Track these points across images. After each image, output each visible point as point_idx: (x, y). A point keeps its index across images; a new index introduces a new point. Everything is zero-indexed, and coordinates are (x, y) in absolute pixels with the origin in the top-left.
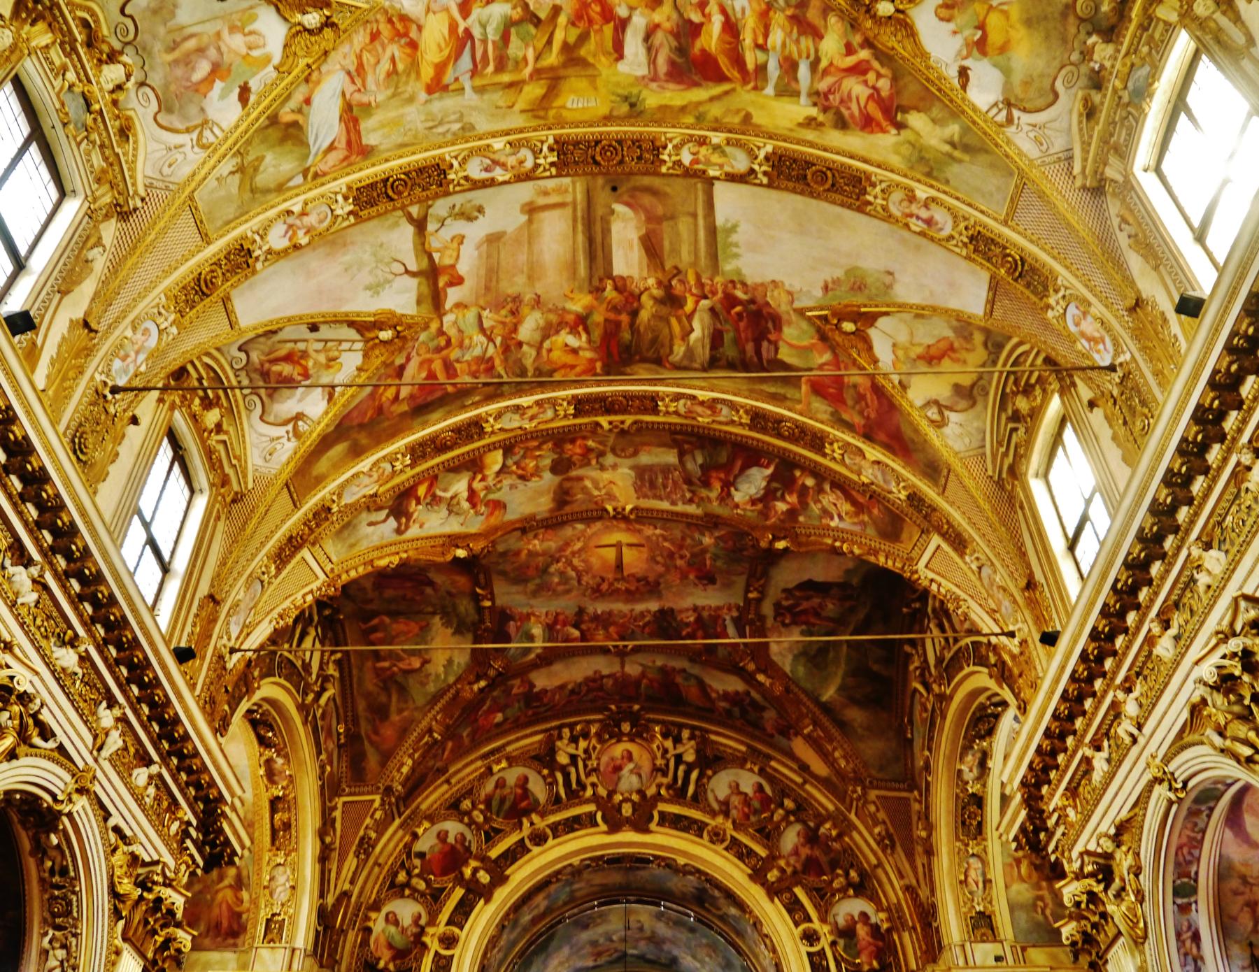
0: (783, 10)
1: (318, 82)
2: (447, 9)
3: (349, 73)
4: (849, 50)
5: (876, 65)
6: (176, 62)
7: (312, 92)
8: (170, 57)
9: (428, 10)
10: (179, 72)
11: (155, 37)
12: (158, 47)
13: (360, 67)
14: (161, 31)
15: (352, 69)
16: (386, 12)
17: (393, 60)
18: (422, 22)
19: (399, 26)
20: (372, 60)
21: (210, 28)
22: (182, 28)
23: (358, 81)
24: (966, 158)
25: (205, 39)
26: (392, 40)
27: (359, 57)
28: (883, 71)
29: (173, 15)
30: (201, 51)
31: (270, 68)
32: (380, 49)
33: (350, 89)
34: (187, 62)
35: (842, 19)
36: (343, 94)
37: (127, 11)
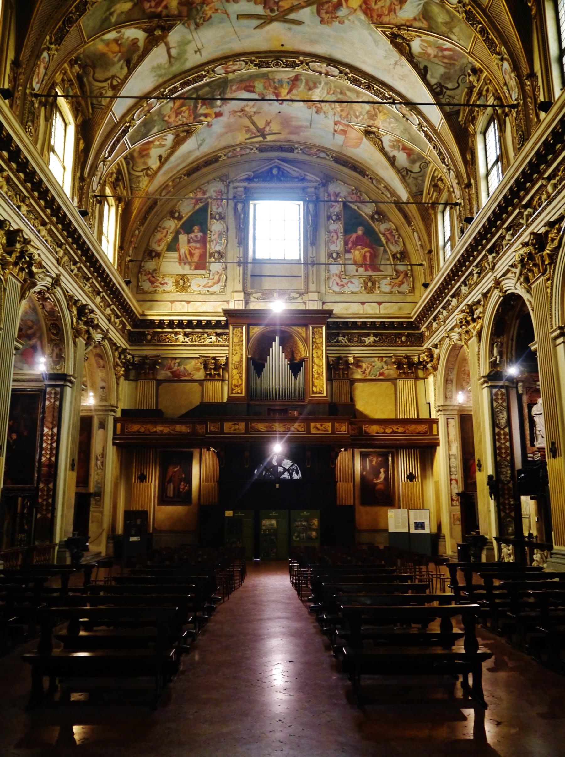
0: (198, 4)
1: (408, 21)
2: (347, 7)
3: (395, 13)
4: (166, 7)
5: (153, 10)
6: (454, 60)
7: (411, 20)
8: (456, 62)
9: (355, 10)
10: (456, 57)
11: (455, 71)
12: (457, 68)
13: (390, 10)
14: (452, 71)
15: (393, 13)
16: (372, 20)
17: (376, 4)
18: (359, 8)
19: (369, 12)
20: (384, 9)
21: (436, 60)
22: (445, 67)
23: (393, 6)
24: (104, 17)
25: (440, 59)
26: (373, 10)
27: (389, 14)
28: (150, 10)
29: (445, 73)
30: (444, 57)
31: (423, 38)
32: (380, 10)
33: (398, 7)
34: (450, 58)
35: (173, 16)
36: (401, 8)
37: (457, 85)
